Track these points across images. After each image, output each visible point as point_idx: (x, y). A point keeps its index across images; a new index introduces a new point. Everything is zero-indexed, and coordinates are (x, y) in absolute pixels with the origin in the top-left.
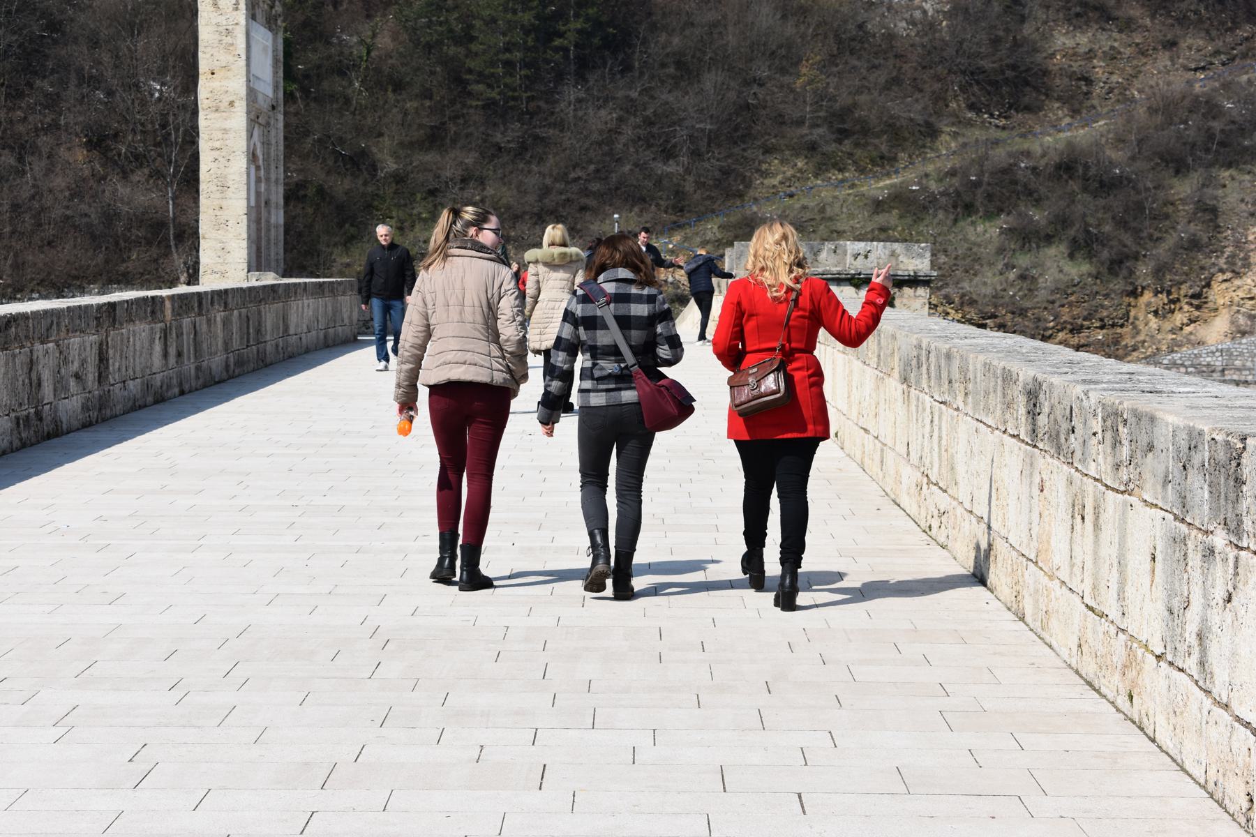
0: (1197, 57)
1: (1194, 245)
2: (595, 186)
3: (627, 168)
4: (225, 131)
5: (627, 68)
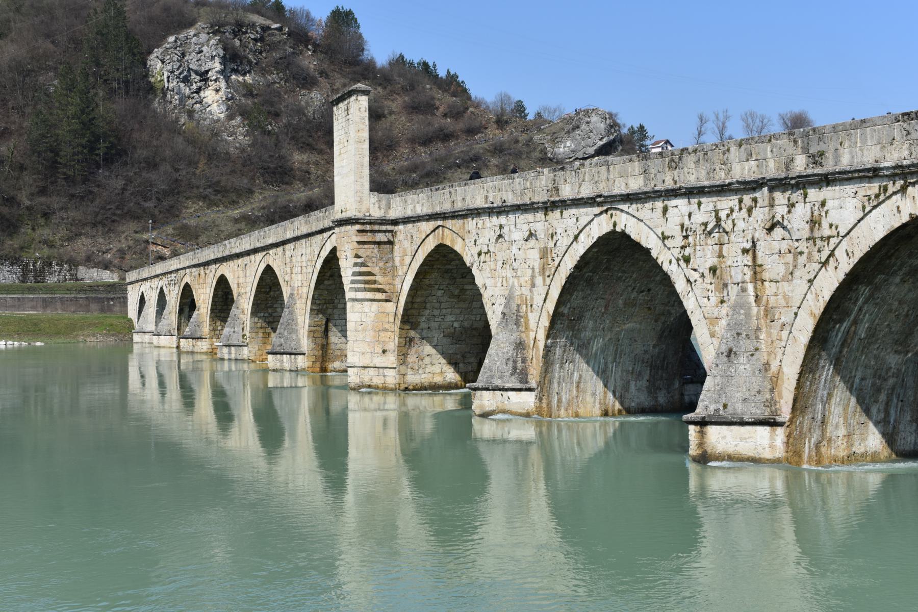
3: (132, 204)
5: (126, 164)
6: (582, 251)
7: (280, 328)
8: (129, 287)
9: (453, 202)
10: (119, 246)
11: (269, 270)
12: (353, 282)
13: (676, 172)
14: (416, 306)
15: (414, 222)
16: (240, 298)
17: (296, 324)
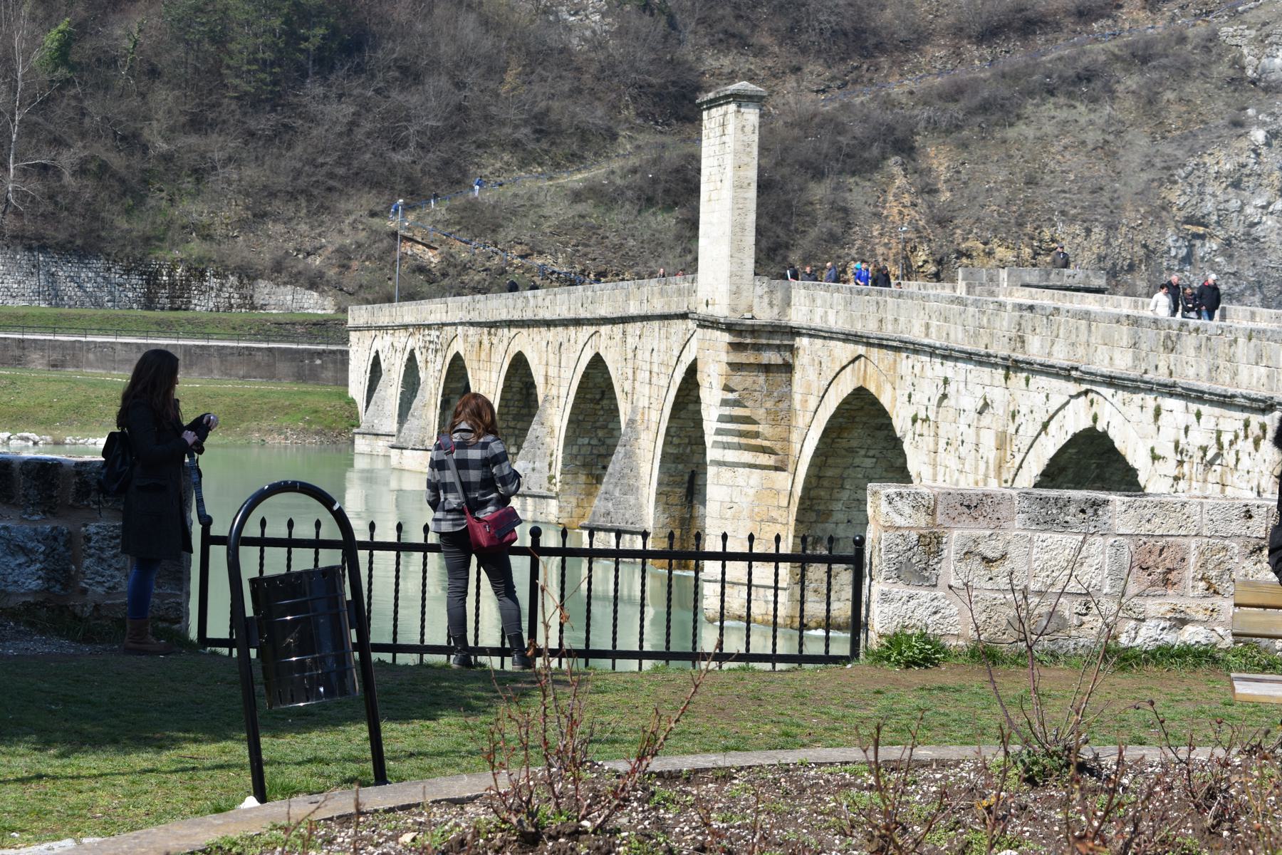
0: (818, 80)
1: (833, 239)
2: (341, 171)
3: (368, 156)
4: (745, 199)
5: (359, 70)
6: (1052, 452)
7: (608, 483)
8: (353, 336)
9: (881, 321)
10: (338, 241)
11: (597, 362)
12: (719, 432)
13: (1172, 356)
14: (826, 483)
15: (825, 338)
16: (547, 405)
17: (637, 477)
